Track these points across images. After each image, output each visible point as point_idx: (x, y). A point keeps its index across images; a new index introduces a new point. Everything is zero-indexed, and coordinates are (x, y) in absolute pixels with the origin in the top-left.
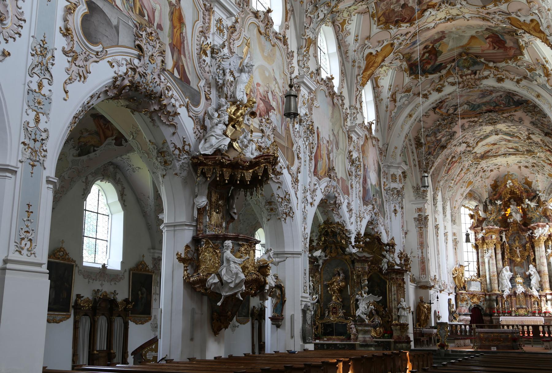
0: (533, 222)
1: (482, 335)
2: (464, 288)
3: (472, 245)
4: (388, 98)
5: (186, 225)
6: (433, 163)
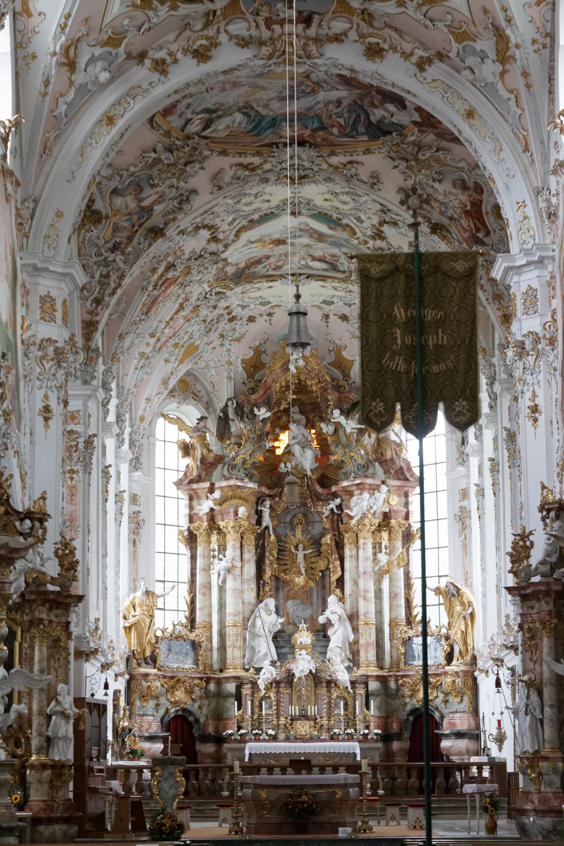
0: (347, 478)
1: (263, 794)
2: (153, 660)
3: (181, 532)
4: (55, 54)
6: (122, 277)
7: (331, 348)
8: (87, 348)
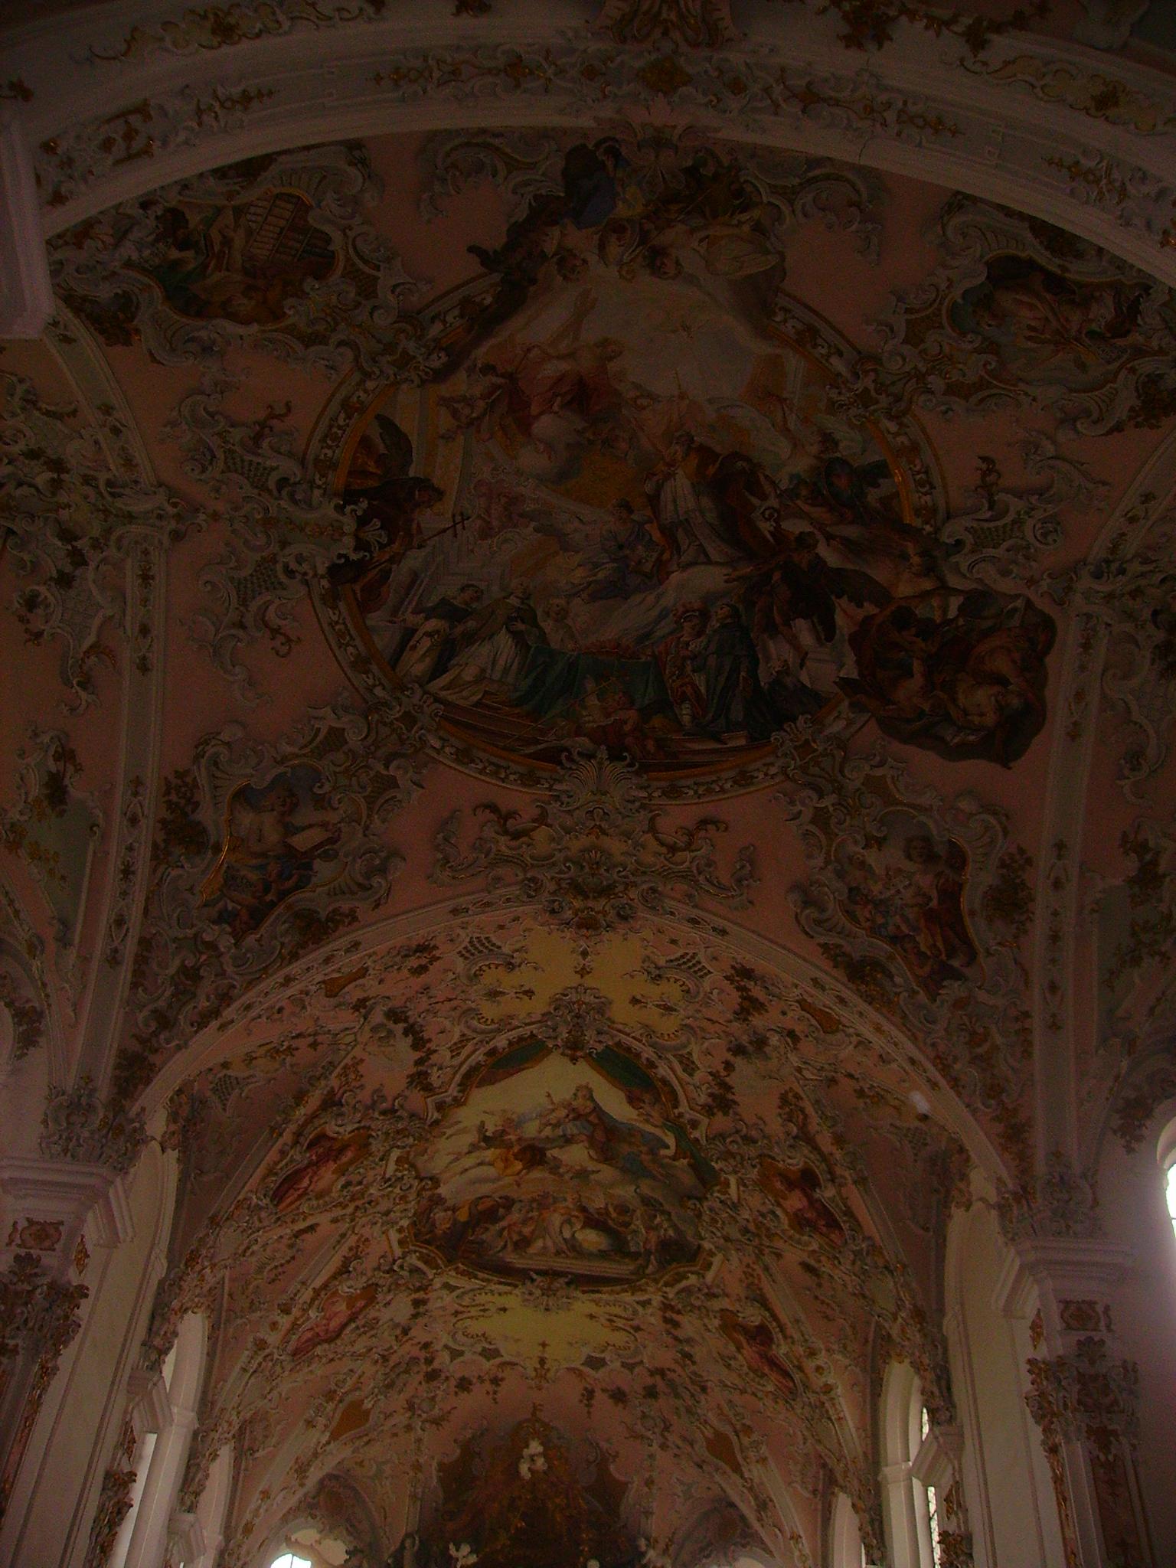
7: (592, 1459)
8: (117, 1106)
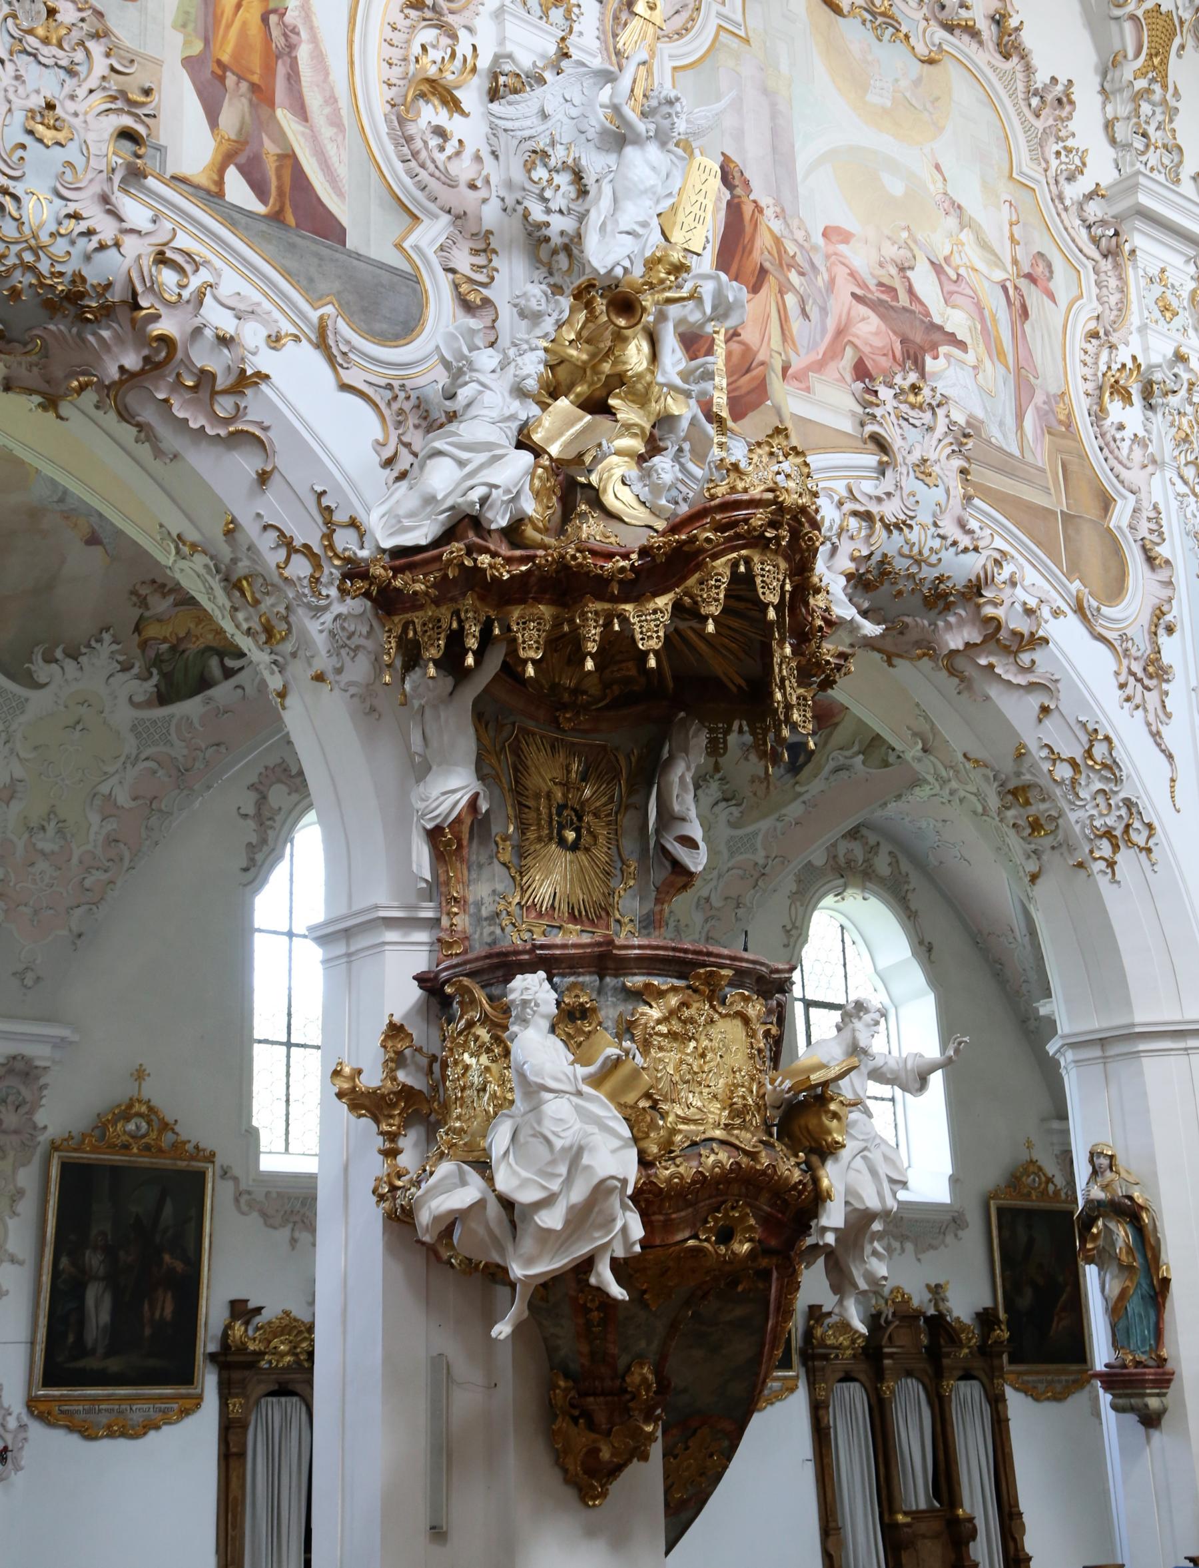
5: (390, 923)
